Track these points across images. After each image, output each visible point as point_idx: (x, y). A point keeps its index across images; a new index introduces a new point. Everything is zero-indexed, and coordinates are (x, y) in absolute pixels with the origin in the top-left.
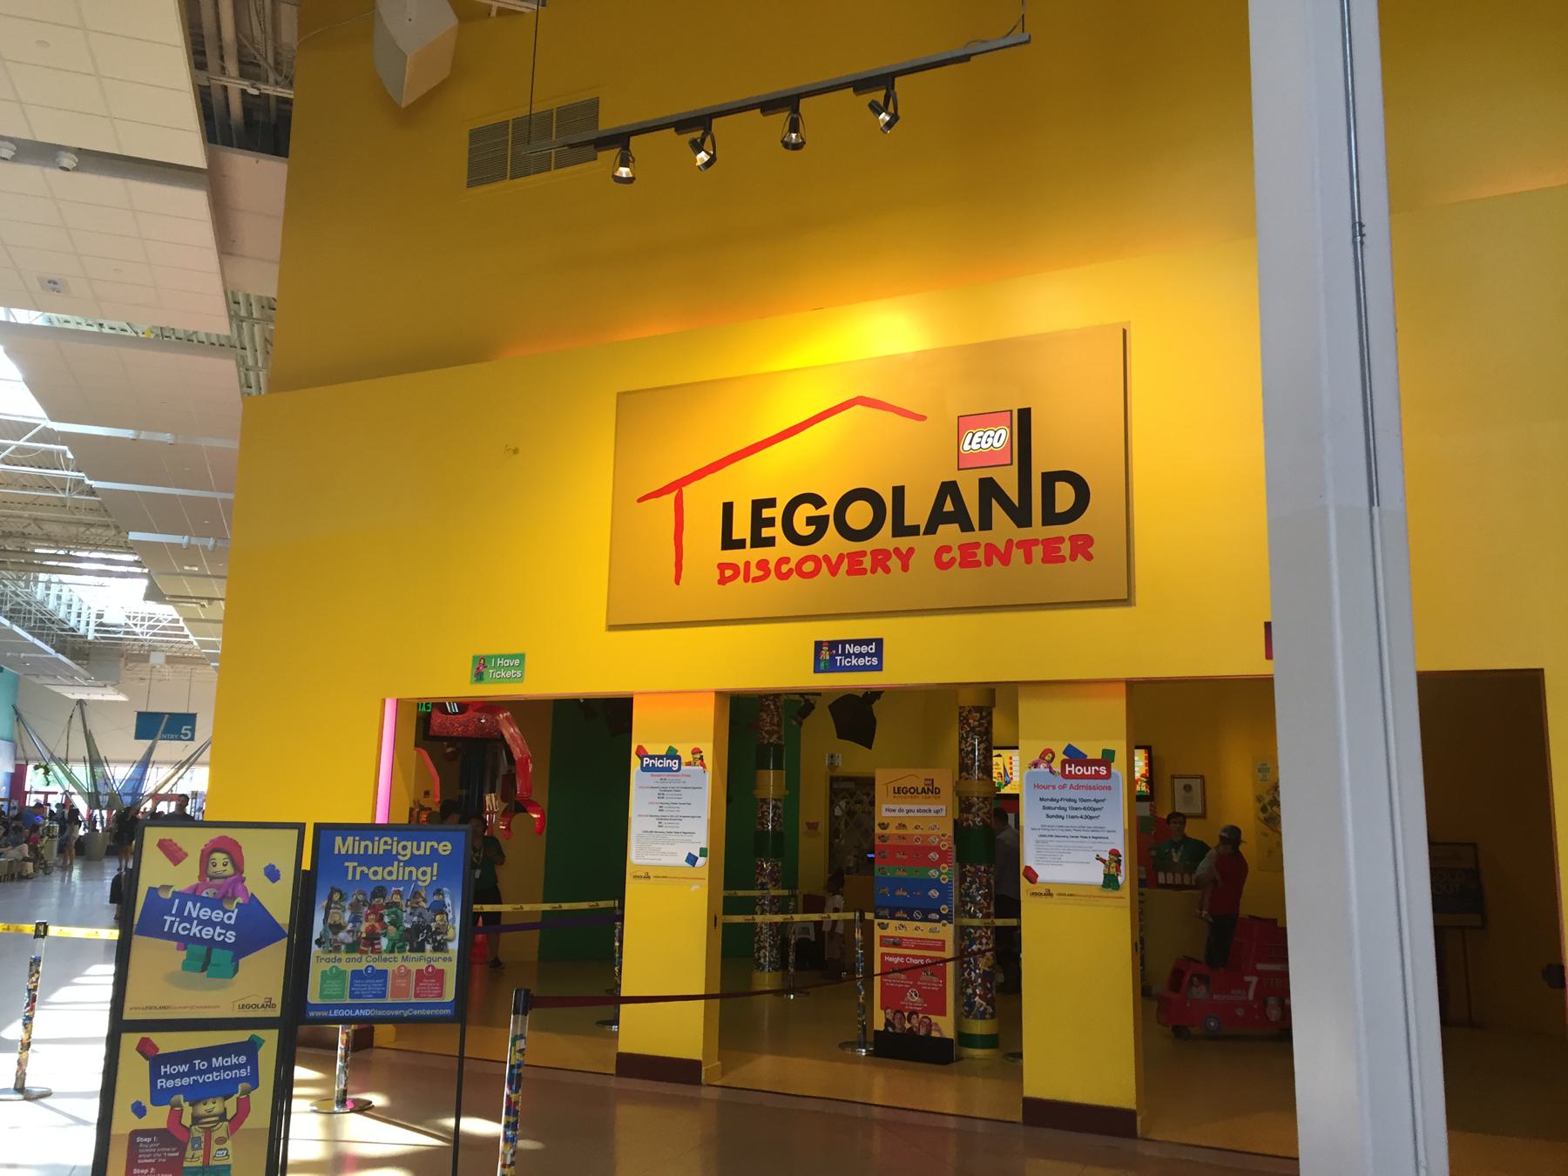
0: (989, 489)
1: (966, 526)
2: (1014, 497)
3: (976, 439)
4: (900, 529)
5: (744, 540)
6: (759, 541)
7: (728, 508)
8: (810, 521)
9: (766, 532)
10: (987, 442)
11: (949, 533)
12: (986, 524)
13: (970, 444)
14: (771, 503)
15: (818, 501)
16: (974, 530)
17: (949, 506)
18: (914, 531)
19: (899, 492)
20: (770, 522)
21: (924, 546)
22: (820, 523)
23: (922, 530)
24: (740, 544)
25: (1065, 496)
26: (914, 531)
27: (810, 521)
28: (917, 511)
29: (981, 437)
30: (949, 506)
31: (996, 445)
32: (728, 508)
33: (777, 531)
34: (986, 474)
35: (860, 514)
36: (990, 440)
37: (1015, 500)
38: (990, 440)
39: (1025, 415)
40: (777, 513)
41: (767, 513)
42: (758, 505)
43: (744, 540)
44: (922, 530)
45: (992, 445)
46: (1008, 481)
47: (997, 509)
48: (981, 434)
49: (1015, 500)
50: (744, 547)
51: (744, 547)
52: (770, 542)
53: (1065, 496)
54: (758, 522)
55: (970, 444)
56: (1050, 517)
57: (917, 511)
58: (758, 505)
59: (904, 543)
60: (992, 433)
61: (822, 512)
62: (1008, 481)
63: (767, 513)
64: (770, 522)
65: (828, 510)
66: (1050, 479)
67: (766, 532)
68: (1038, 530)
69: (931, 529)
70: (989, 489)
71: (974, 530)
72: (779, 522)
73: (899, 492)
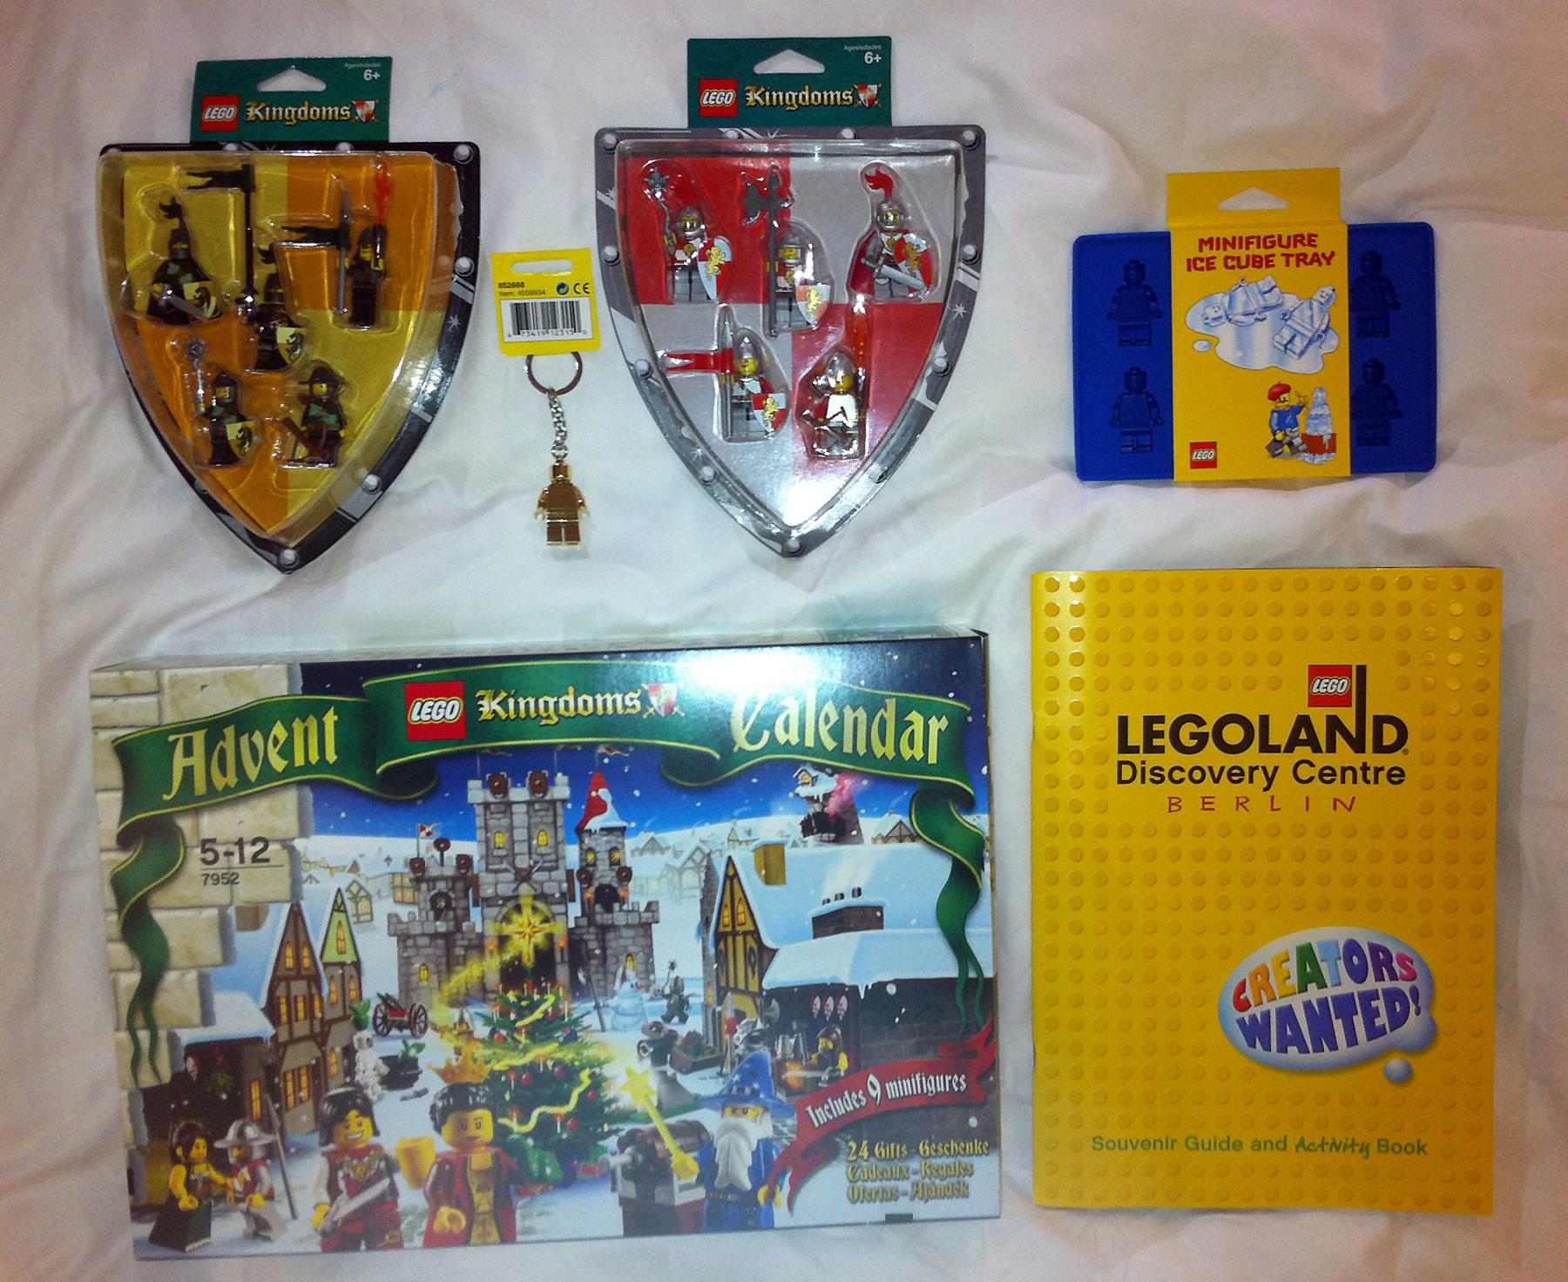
0: (1334, 724)
1: (1317, 749)
2: (1353, 731)
4: (1266, 747)
5: (1138, 747)
6: (1150, 749)
7: (1123, 722)
8: (1193, 736)
9: (1156, 742)
11: (1303, 752)
12: (1332, 748)
14: (1161, 719)
15: (1199, 721)
17: (1303, 736)
18: (1276, 749)
20: (1160, 734)
21: (1285, 761)
22: (1202, 740)
23: (1282, 749)
24: (1135, 750)
25: (1390, 735)
26: (1276, 749)
27: (1193, 736)
28: (1279, 736)
30: (1303, 736)
31: (1339, 691)
32: (1123, 722)
33: (1165, 742)
35: (1233, 734)
36: (1335, 686)
37: (1353, 733)
38: (1335, 686)
39: (1362, 670)
40: (1165, 728)
41: (1156, 727)
42: (1149, 721)
43: (1138, 747)
44: (1282, 749)
46: (1348, 716)
47: (1340, 740)
49: (1353, 733)
50: (1138, 752)
51: (1138, 752)
52: (1161, 750)
53: (1390, 735)
54: (1149, 734)
56: (1379, 748)
57: (1279, 736)
58: (1149, 721)
59: (1270, 760)
60: (1337, 681)
61: (1203, 729)
62: (1348, 716)
63: (1156, 727)
64: (1160, 734)
65: (1208, 728)
66: (1379, 721)
67: (1156, 742)
68: (1372, 758)
69: (1290, 748)
70: (1334, 724)
73: (1264, 720)
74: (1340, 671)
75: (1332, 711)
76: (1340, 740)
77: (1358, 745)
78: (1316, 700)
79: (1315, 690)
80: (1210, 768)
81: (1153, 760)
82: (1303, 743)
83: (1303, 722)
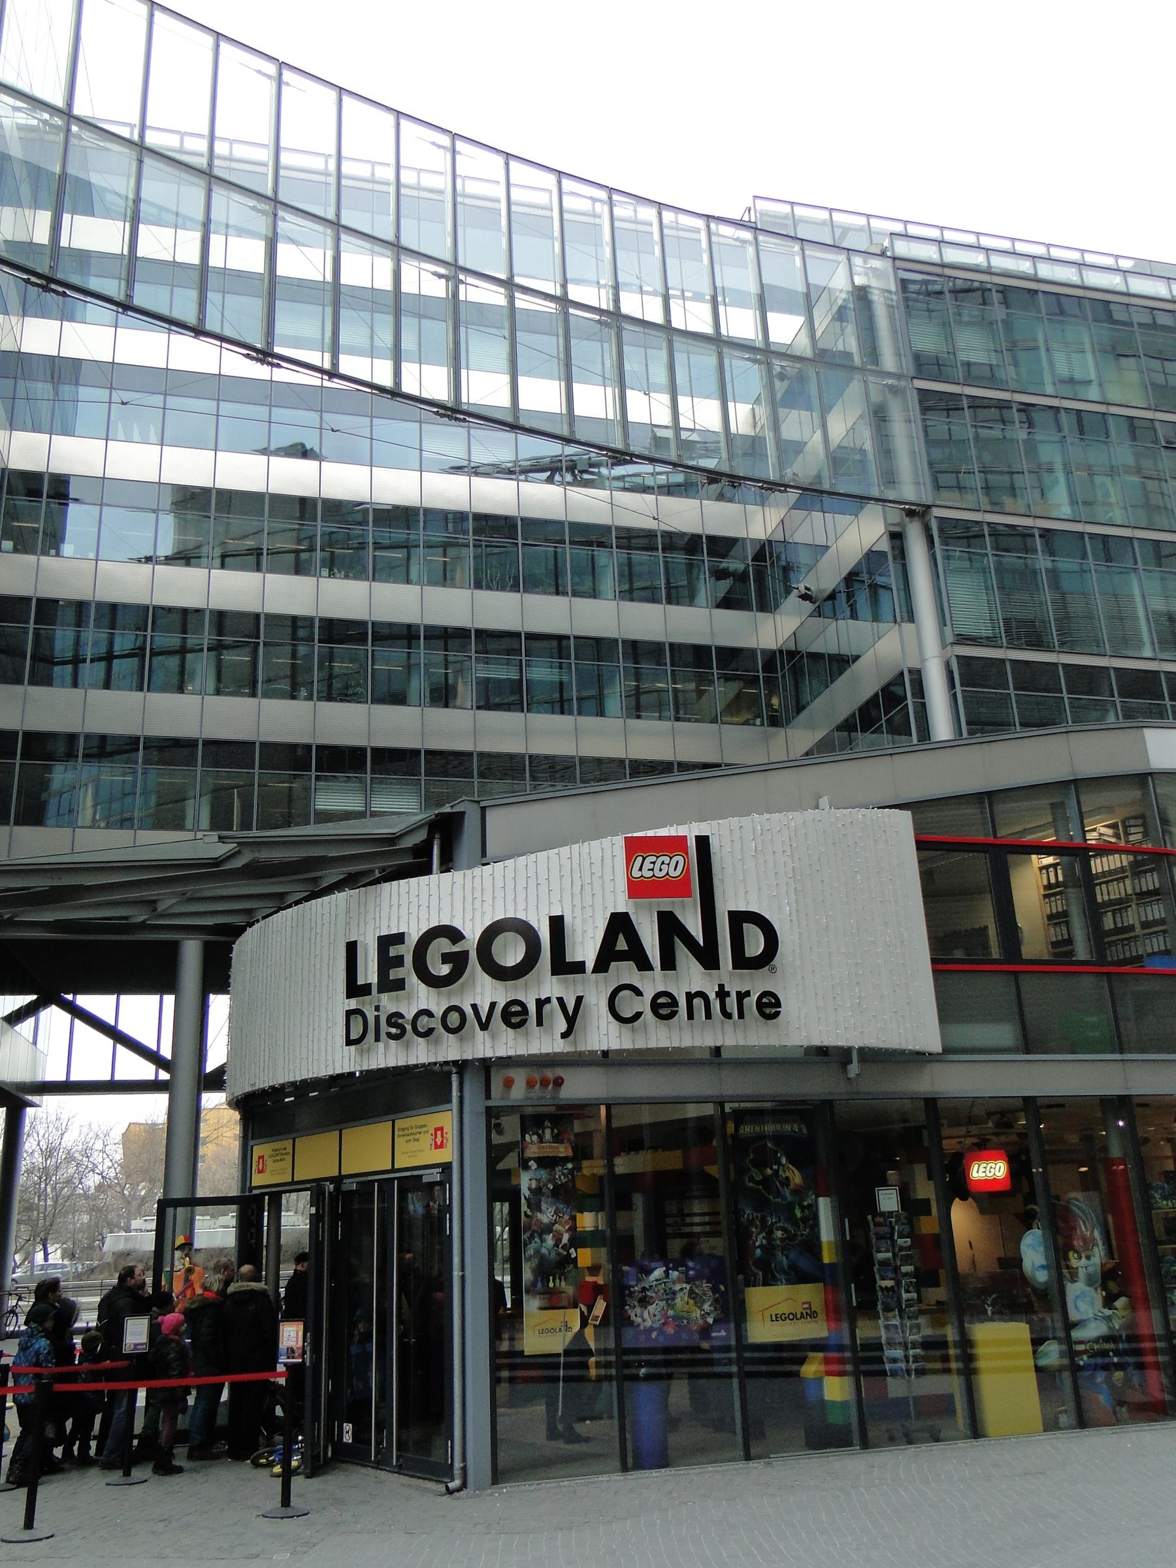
1: (644, 964)
3: (647, 865)
4: (563, 966)
9: (394, 974)
10: (661, 870)
11: (624, 972)
12: (669, 962)
13: (640, 869)
14: (399, 938)
16: (651, 968)
17: (622, 945)
19: (557, 924)
20: (399, 961)
23: (590, 965)
28: (585, 947)
29: (654, 863)
30: (622, 945)
33: (407, 971)
34: (666, 904)
35: (511, 953)
36: (665, 867)
38: (665, 867)
40: (407, 951)
41: (393, 951)
45: (668, 874)
47: (679, 945)
48: (653, 859)
52: (400, 985)
55: (640, 869)
57: (585, 947)
60: (667, 859)
63: (393, 951)
64: (399, 961)
67: (394, 974)
70: (669, 926)
71: (651, 968)
72: (409, 960)
73: (557, 924)
74: (676, 845)
75: (666, 904)
76: (683, 954)
77: (708, 957)
78: (637, 889)
79: (636, 873)
80: (474, 1007)
81: (389, 1003)
82: (622, 956)
83: (619, 924)
